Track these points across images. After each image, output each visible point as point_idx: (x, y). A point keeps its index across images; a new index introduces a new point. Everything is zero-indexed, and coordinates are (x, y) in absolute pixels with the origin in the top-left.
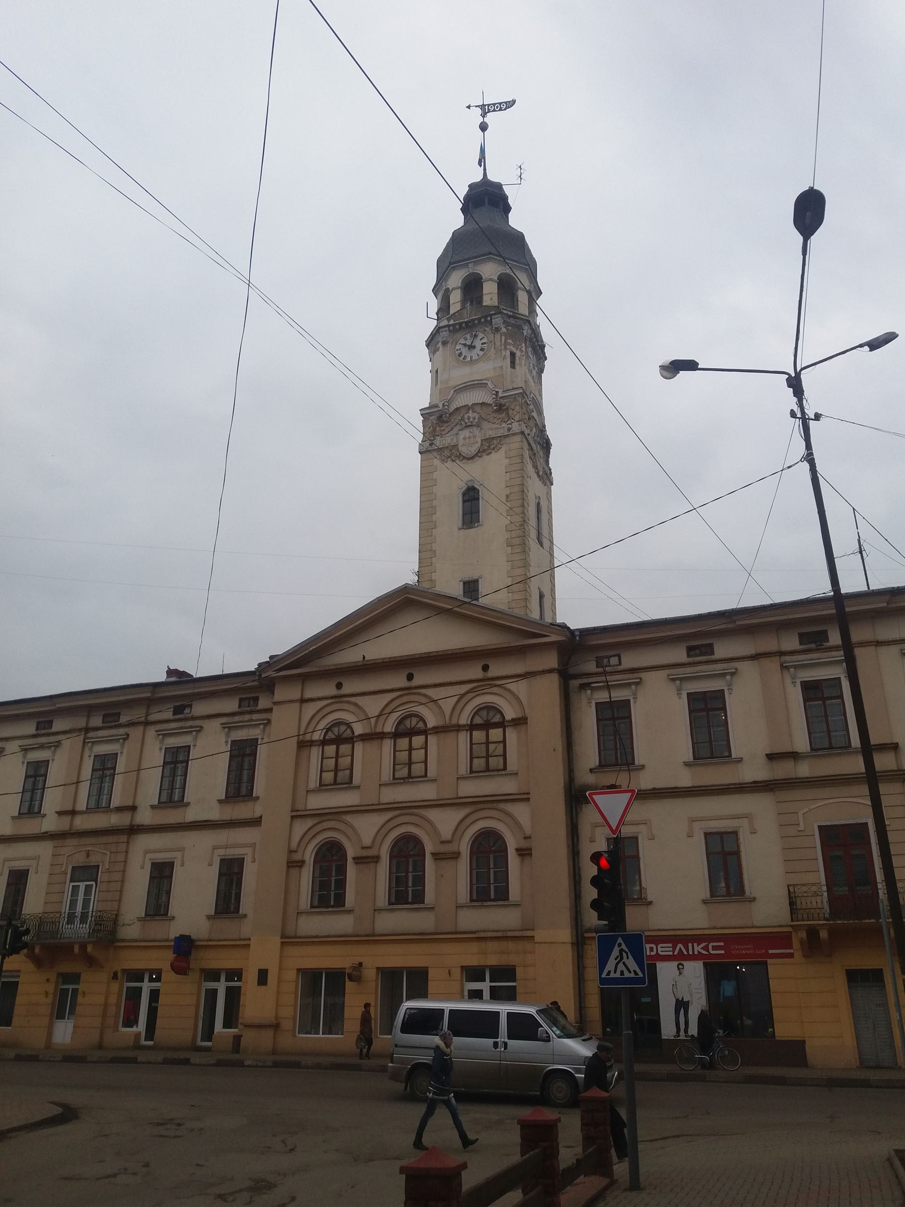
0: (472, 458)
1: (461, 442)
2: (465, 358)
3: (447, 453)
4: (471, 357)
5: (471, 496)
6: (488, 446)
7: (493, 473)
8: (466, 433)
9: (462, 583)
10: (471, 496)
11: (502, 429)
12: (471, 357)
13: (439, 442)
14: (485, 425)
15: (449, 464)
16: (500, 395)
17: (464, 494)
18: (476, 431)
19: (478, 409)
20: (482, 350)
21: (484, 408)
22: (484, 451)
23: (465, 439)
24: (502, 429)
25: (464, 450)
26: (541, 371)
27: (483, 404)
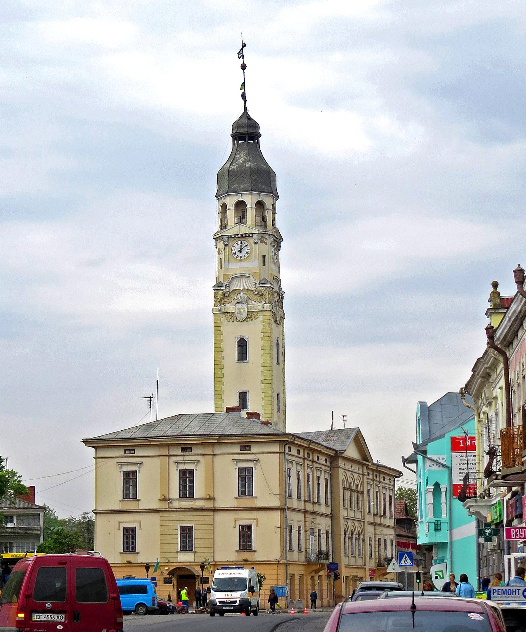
0: (243, 321)
1: (236, 311)
2: (237, 257)
3: (228, 315)
4: (241, 257)
5: (242, 344)
6: (251, 315)
7: (254, 333)
8: (239, 306)
9: (238, 394)
10: (242, 344)
11: (258, 306)
12: (241, 257)
13: (225, 308)
14: (250, 302)
15: (231, 322)
16: (258, 285)
17: (238, 342)
18: (245, 306)
19: (246, 292)
20: (247, 253)
21: (249, 292)
22: (249, 318)
23: (239, 309)
24: (258, 306)
25: (239, 316)
26: (279, 250)
27: (248, 290)
